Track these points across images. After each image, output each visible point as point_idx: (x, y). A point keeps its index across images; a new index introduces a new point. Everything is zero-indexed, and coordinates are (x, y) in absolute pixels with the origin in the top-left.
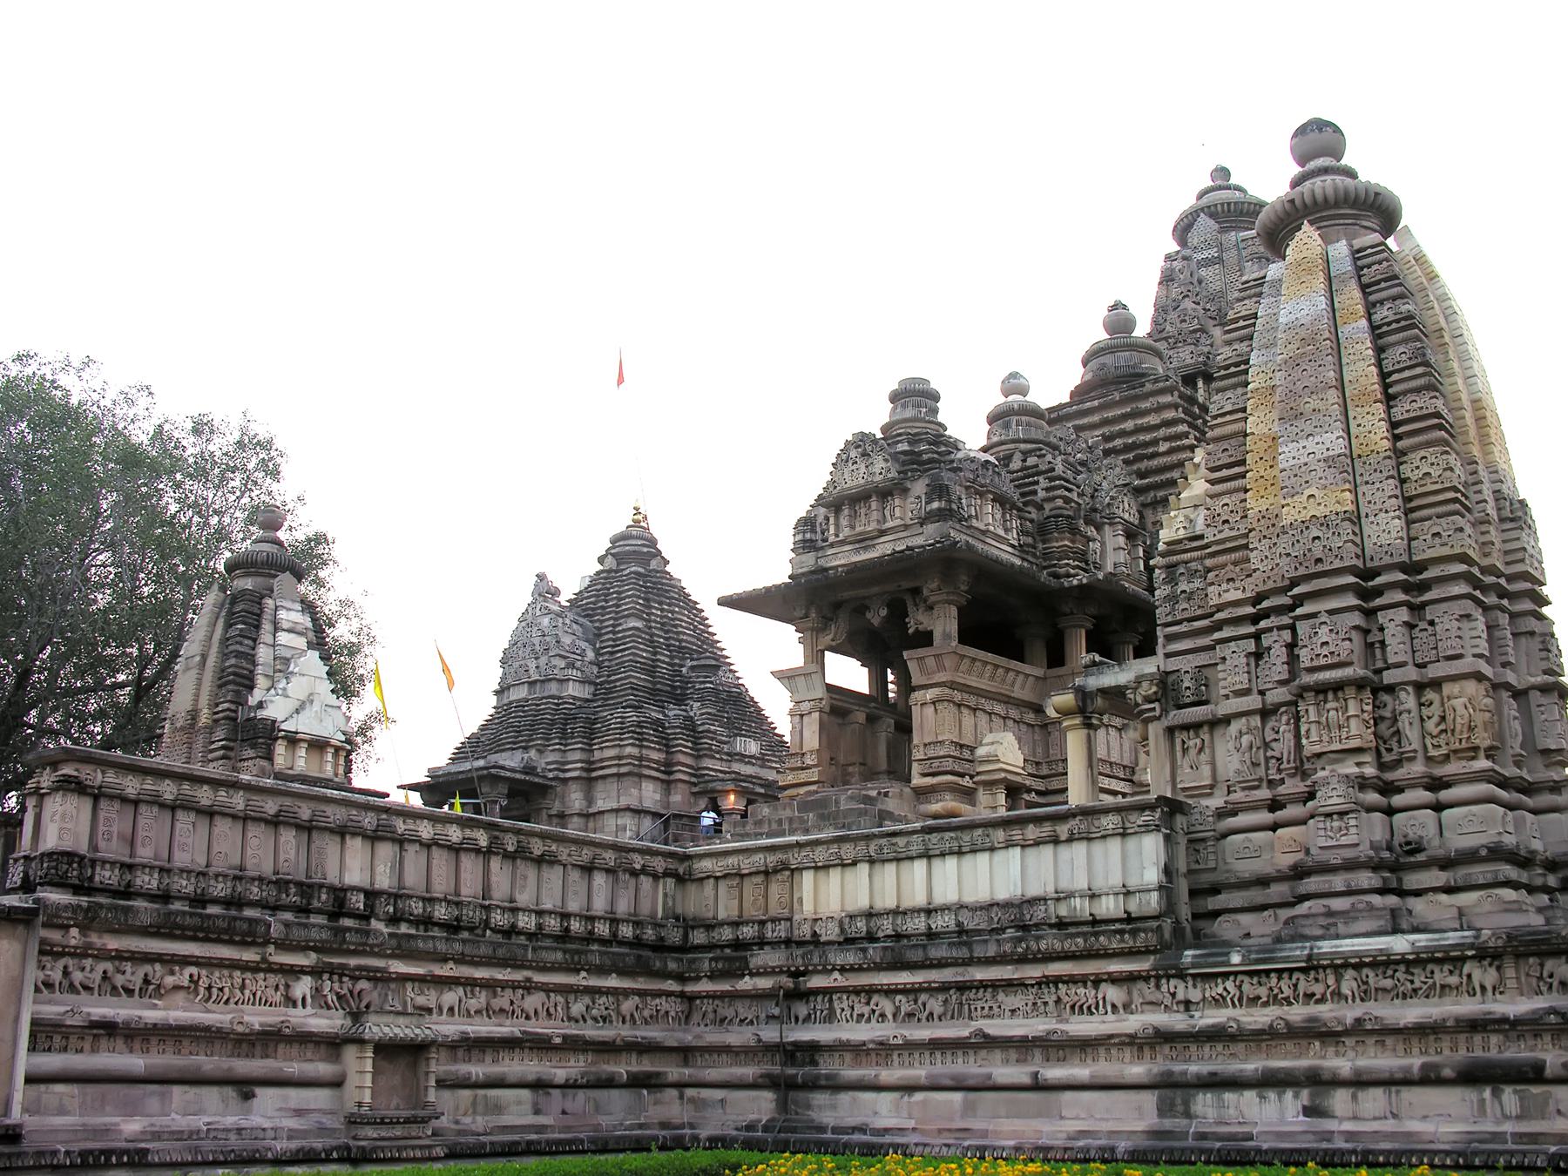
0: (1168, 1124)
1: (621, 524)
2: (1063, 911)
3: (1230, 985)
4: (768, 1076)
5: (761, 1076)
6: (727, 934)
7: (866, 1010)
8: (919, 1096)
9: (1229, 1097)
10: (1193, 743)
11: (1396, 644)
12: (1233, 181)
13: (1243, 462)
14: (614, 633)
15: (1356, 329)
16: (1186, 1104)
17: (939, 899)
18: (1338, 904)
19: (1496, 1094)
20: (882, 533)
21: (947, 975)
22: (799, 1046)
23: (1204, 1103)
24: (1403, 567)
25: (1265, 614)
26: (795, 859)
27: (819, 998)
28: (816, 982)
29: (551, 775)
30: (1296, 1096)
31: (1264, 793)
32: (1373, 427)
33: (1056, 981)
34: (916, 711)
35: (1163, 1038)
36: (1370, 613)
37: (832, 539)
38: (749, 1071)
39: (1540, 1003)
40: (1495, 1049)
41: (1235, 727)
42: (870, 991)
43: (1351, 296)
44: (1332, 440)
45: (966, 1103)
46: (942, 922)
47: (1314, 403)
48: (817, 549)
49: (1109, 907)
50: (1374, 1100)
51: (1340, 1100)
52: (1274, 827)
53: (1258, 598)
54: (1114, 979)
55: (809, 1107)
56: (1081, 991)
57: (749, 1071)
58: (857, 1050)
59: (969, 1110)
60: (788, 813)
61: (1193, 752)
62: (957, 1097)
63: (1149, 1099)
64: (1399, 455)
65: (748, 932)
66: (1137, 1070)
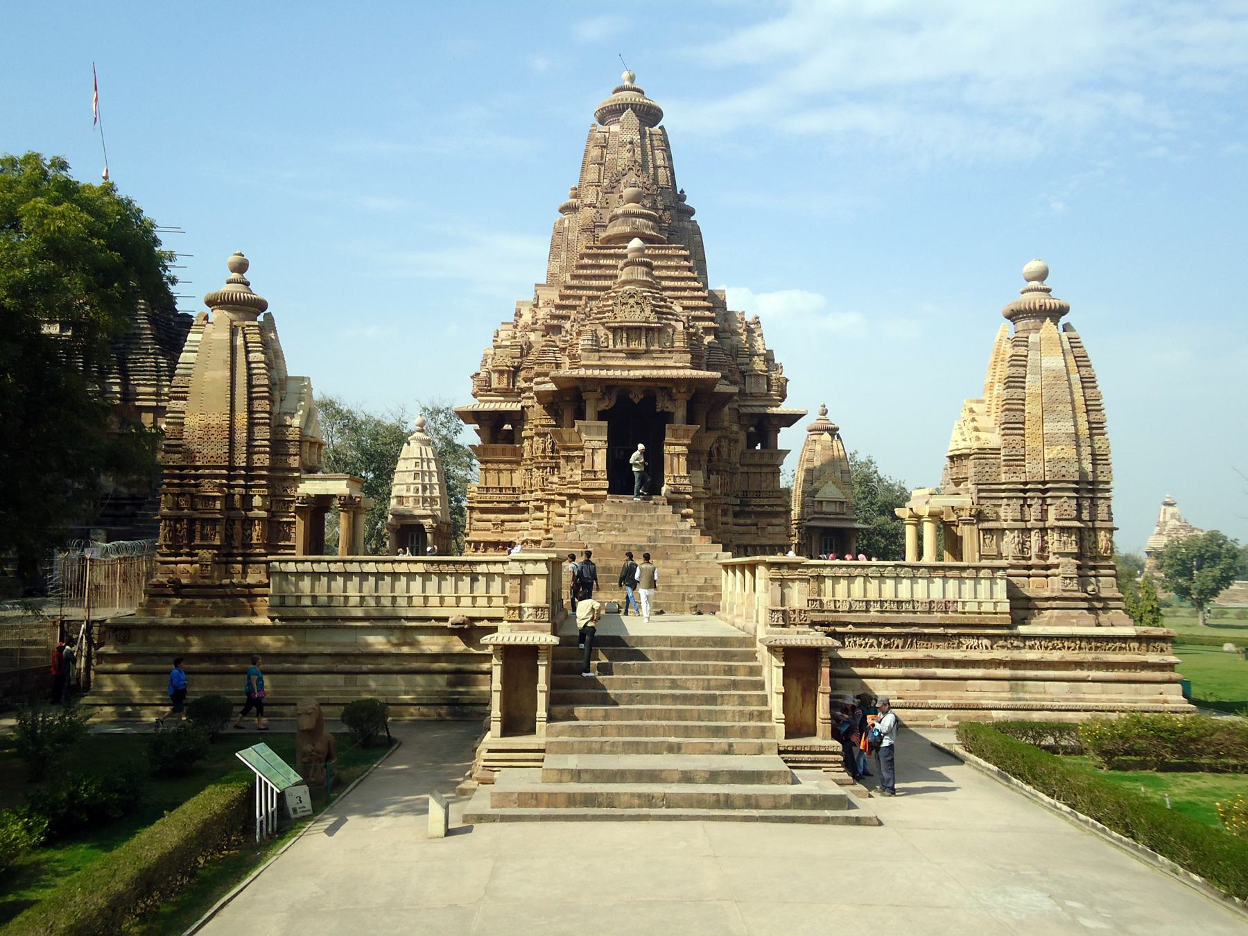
11: (1085, 515)
13: (1023, 423)
20: (647, 352)
25: (1029, 490)
26: (826, 572)
33: (959, 635)
34: (667, 458)
37: (611, 347)
42: (865, 635)
45: (922, 685)
52: (1029, 576)
53: (1026, 483)
54: (987, 636)
59: (923, 688)
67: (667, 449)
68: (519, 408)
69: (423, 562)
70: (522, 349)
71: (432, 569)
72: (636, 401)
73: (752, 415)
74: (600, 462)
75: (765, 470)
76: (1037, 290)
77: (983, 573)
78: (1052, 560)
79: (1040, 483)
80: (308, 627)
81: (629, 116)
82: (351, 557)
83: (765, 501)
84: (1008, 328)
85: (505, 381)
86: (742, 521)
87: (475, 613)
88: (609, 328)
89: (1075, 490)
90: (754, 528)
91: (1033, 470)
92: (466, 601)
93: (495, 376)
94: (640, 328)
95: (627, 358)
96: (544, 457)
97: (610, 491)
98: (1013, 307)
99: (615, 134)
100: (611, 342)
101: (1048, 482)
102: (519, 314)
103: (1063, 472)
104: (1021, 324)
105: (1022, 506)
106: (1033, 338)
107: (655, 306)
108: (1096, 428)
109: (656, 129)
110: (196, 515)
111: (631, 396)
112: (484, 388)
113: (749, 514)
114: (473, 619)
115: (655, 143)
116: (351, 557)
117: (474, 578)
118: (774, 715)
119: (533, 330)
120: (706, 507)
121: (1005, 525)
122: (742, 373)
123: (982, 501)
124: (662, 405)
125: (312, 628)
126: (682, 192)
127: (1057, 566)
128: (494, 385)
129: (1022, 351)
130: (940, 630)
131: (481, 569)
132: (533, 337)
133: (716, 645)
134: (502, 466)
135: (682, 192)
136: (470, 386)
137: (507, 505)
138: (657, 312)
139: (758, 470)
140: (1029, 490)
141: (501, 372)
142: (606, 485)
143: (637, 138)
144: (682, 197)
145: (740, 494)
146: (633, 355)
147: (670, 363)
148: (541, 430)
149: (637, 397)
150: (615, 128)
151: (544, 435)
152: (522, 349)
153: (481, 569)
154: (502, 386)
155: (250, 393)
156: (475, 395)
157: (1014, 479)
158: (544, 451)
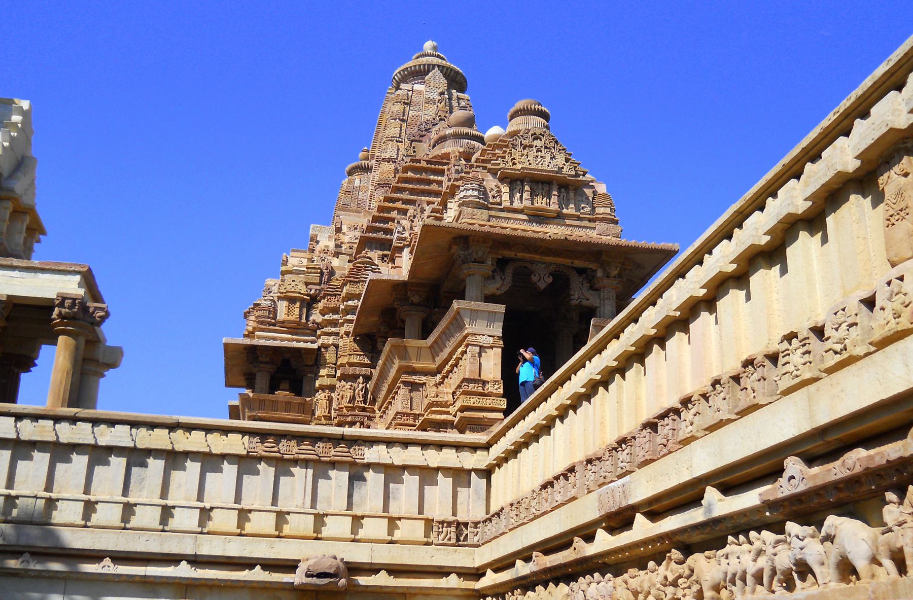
37: (506, 204)
68: (315, 346)
69: (244, 432)
70: (322, 273)
71: (260, 449)
72: (542, 285)
74: (492, 366)
81: (436, 76)
82: (72, 411)
85: (297, 311)
87: (359, 554)
88: (502, 180)
92: (337, 526)
93: (282, 306)
95: (529, 221)
96: (353, 409)
99: (420, 92)
100: (506, 197)
111: (534, 278)
114: (354, 569)
116: (72, 411)
117: (357, 472)
119: (337, 255)
128: (281, 315)
131: (373, 454)
132: (335, 262)
141: (292, 300)
146: (538, 217)
148: (351, 371)
150: (417, 87)
151: (354, 378)
152: (322, 273)
153: (373, 454)
154: (291, 318)
158: (353, 399)
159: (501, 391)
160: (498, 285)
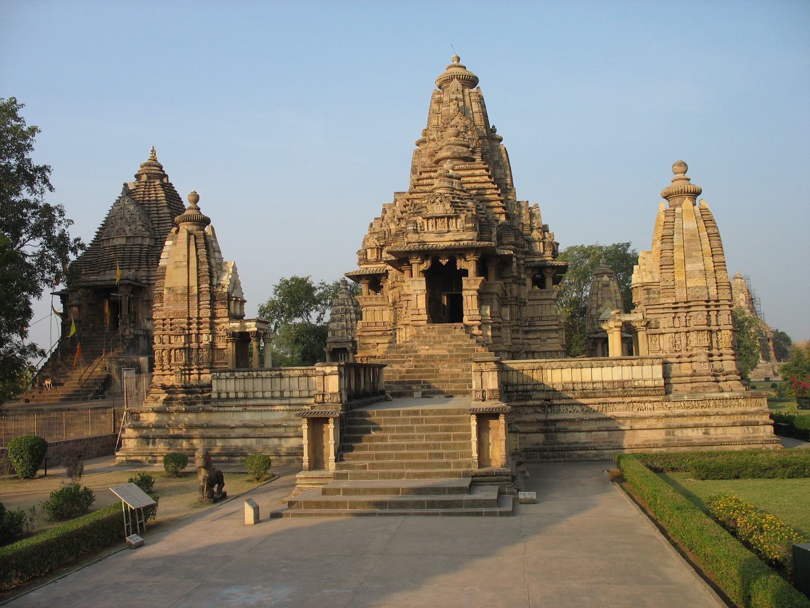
0: (668, 437)
1: (146, 159)
2: (636, 384)
3: (682, 403)
4: (542, 429)
5: (540, 430)
6: (521, 388)
7: (572, 410)
8: (593, 433)
9: (684, 431)
10: (654, 338)
12: (461, 63)
14: (158, 214)
15: (704, 234)
16: (673, 433)
17: (594, 379)
18: (705, 384)
19: (748, 429)
20: (449, 232)
21: (601, 400)
22: (551, 421)
23: (678, 433)
24: (716, 301)
27: (555, 407)
28: (555, 402)
29: (144, 282)
30: (701, 430)
31: (677, 354)
32: (709, 261)
33: (632, 402)
34: (464, 297)
35: (667, 416)
36: (708, 311)
38: (534, 428)
39: (756, 408)
40: (746, 418)
41: (667, 336)
43: (701, 223)
44: (700, 266)
46: (599, 386)
47: (695, 254)
48: (418, 233)
49: (649, 383)
50: (720, 431)
51: (712, 431)
55: (556, 438)
56: (641, 405)
57: (534, 428)
58: (572, 421)
60: (434, 334)
61: (653, 342)
62: (606, 433)
63: (663, 432)
64: (715, 271)
65: (529, 387)
66: (660, 425)
67: (464, 293)
73: (534, 268)
75: (544, 302)
76: (680, 179)
77: (646, 361)
78: (694, 352)
79: (685, 303)
80: (234, 411)
81: (456, 84)
83: (545, 323)
84: (664, 205)
86: (530, 336)
89: (707, 306)
90: (538, 340)
91: (681, 294)
94: (443, 217)
95: (437, 237)
97: (428, 322)
98: (666, 191)
100: (426, 227)
101: (690, 302)
102: (385, 211)
103: (698, 295)
104: (672, 202)
105: (674, 318)
106: (678, 210)
107: (452, 202)
108: (720, 266)
109: (475, 89)
110: (172, 346)
112: (364, 260)
113: (536, 331)
115: (472, 98)
118: (473, 455)
120: (493, 329)
121: (663, 331)
122: (527, 240)
123: (648, 316)
124: (461, 264)
125: (237, 411)
126: (493, 127)
127: (696, 355)
129: (671, 219)
130: (620, 400)
133: (435, 414)
134: (376, 308)
135: (493, 127)
136: (356, 258)
137: (380, 333)
138: (454, 206)
139: (540, 302)
140: (689, 307)
142: (426, 317)
143: (460, 96)
144: (494, 130)
145: (529, 319)
146: (440, 234)
147: (464, 237)
149: (444, 262)
155: (198, 273)
156: (360, 265)
157: (669, 301)
159: (425, 312)
160: (425, 266)
